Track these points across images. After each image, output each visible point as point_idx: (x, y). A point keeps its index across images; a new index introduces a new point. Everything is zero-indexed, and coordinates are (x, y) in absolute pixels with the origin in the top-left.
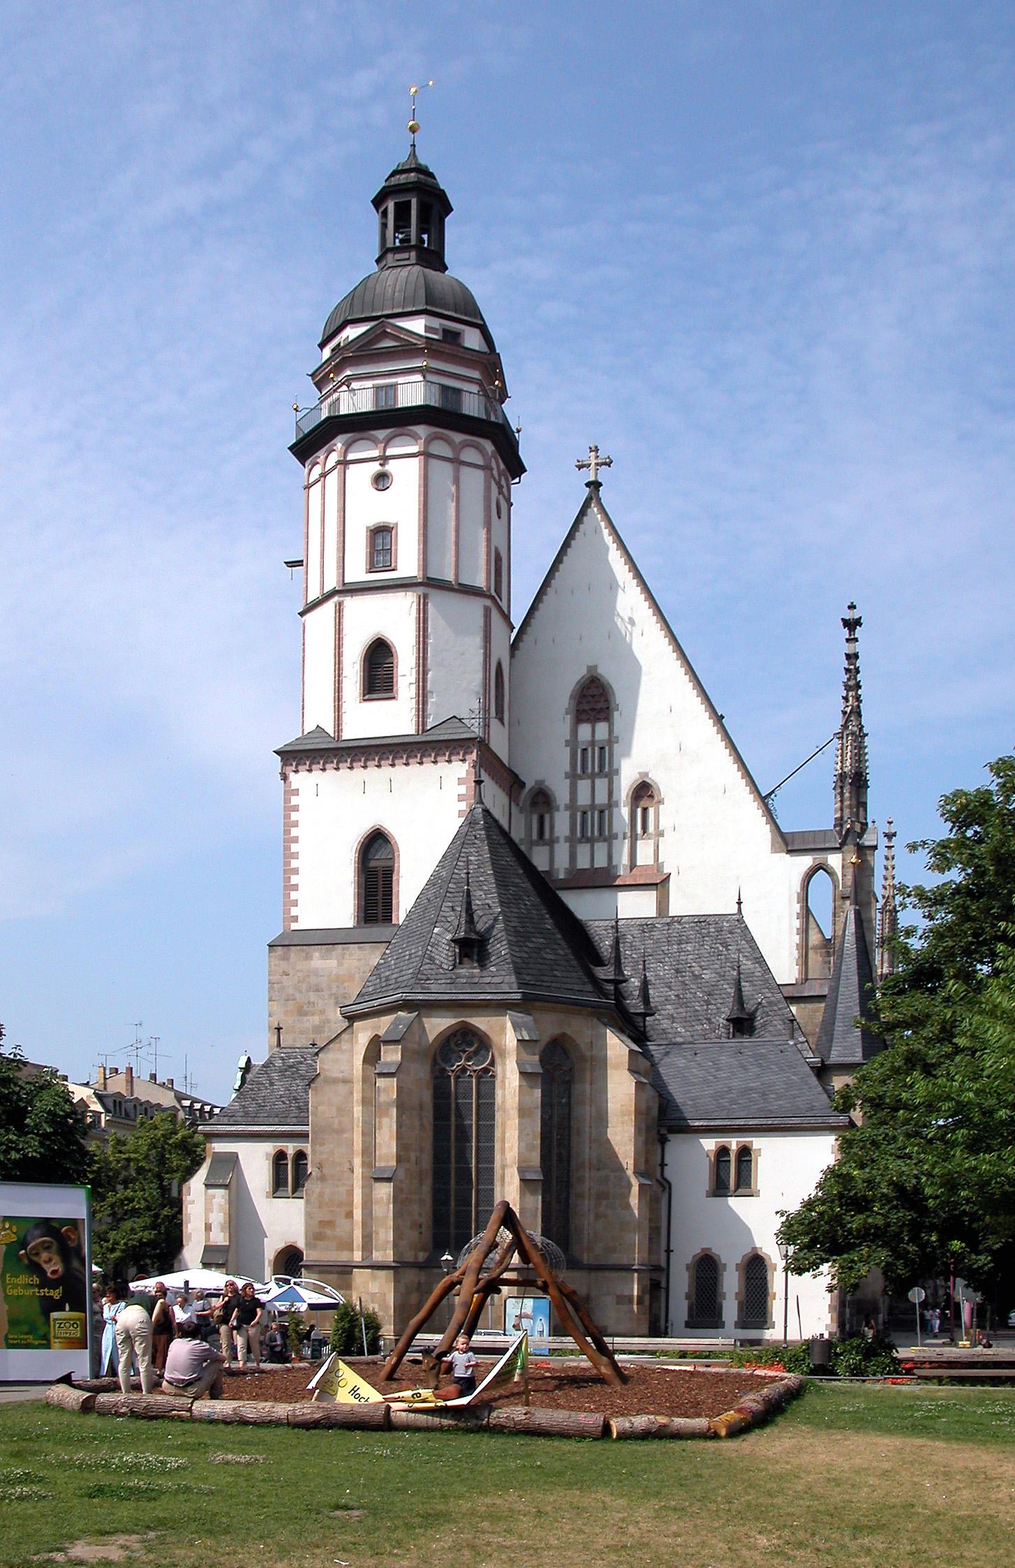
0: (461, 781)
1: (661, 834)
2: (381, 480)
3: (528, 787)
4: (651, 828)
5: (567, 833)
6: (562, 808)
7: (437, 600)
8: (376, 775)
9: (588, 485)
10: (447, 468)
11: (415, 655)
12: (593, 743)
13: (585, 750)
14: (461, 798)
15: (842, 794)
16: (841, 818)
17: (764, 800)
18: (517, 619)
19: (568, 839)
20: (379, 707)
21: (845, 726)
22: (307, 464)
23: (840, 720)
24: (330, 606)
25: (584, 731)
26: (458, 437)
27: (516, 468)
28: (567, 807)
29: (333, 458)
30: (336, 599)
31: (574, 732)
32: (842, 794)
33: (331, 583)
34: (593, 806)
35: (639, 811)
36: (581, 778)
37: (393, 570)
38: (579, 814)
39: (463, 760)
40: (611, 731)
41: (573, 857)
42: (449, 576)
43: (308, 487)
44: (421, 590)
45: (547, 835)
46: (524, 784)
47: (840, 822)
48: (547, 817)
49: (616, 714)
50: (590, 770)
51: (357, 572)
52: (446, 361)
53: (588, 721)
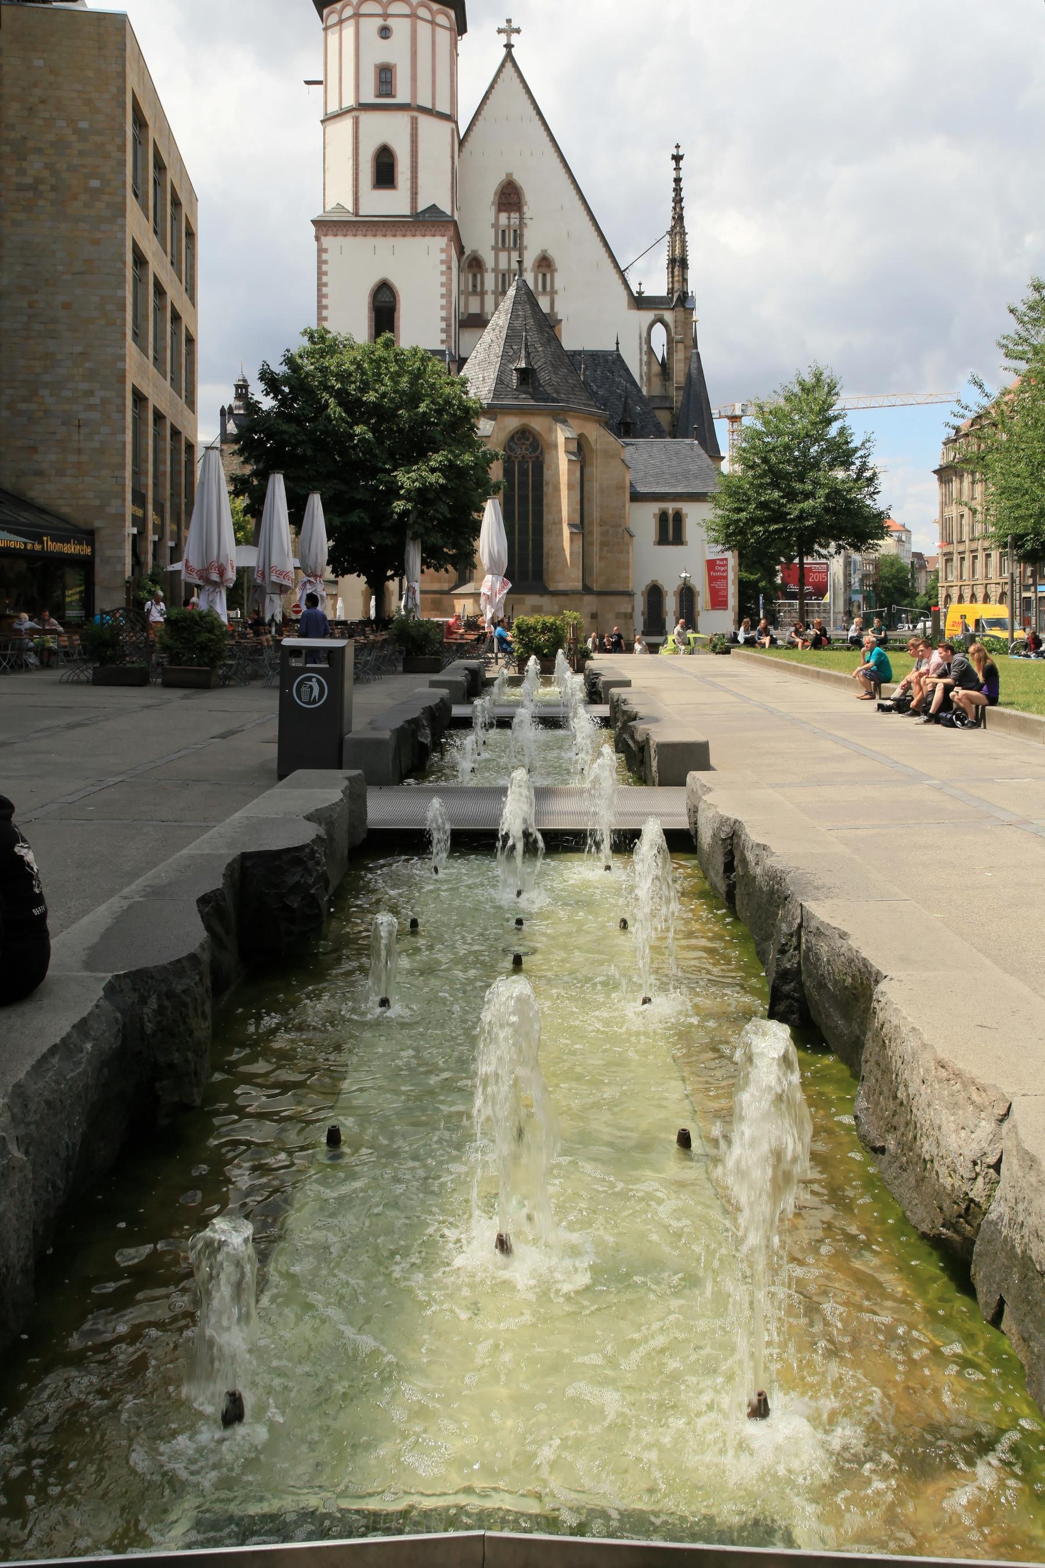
0: (442, 251)
1: (553, 292)
2: (385, 32)
4: (548, 288)
5: (493, 288)
6: (490, 270)
7: (424, 120)
8: (383, 244)
9: (505, 46)
10: (429, 26)
12: (509, 226)
13: (504, 231)
15: (673, 272)
16: (673, 288)
17: (621, 273)
19: (494, 293)
20: (384, 194)
21: (673, 227)
22: (325, 12)
23: (669, 223)
24: (347, 123)
25: (503, 217)
28: (493, 270)
29: (348, 12)
30: (354, 113)
31: (497, 218)
32: (673, 272)
33: (349, 101)
34: (509, 270)
35: (540, 276)
37: (394, 97)
38: (500, 276)
40: (521, 218)
42: (430, 106)
43: (326, 29)
44: (415, 114)
45: (479, 289)
47: (671, 291)
48: (479, 276)
49: (525, 209)
51: (369, 96)
53: (506, 211)
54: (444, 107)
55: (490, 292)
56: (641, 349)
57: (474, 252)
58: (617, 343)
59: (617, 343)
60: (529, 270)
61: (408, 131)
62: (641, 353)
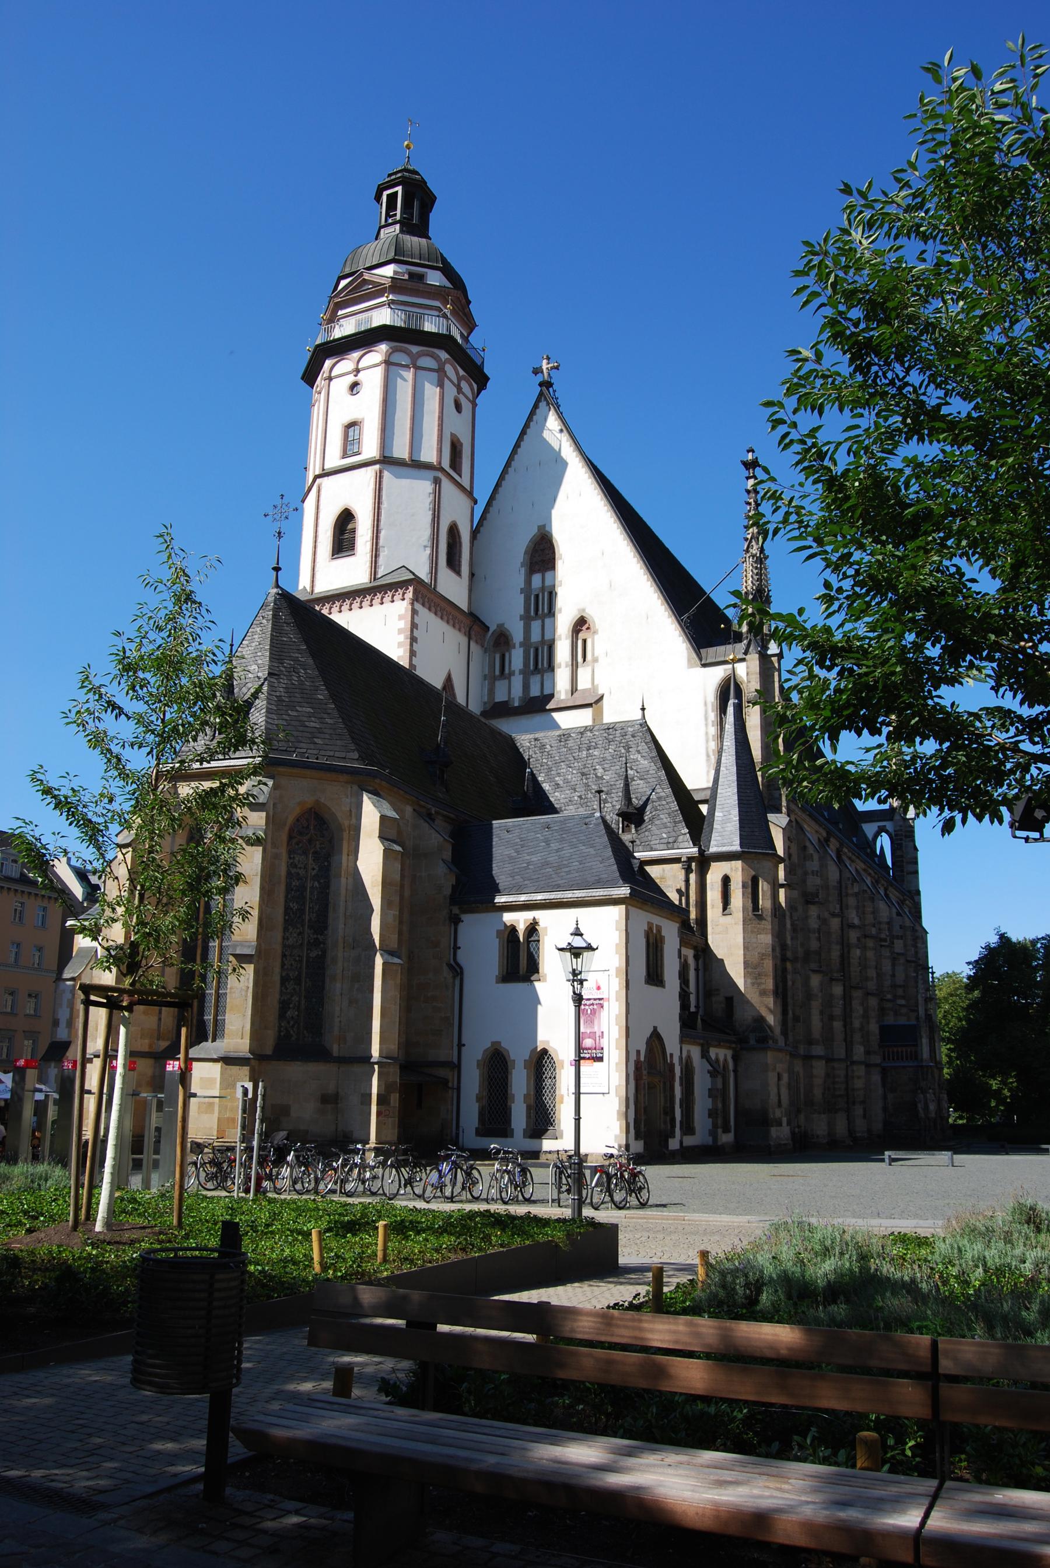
0: (400, 618)
1: (595, 660)
3: (491, 630)
6: (517, 645)
11: (371, 518)
12: (543, 588)
13: (537, 596)
14: (400, 631)
18: (482, 495)
19: (521, 672)
26: (415, 349)
27: (480, 380)
28: (521, 645)
31: (528, 582)
35: (580, 643)
36: (534, 619)
37: (358, 453)
38: (532, 651)
39: (403, 599)
41: (526, 687)
45: (507, 671)
46: (488, 628)
50: (540, 612)
52: (410, 295)
53: (539, 571)
54: (429, 454)
55: (517, 672)
56: (706, 719)
57: (501, 626)
58: (643, 709)
59: (643, 709)
60: (563, 637)
61: (372, 486)
62: (706, 725)
